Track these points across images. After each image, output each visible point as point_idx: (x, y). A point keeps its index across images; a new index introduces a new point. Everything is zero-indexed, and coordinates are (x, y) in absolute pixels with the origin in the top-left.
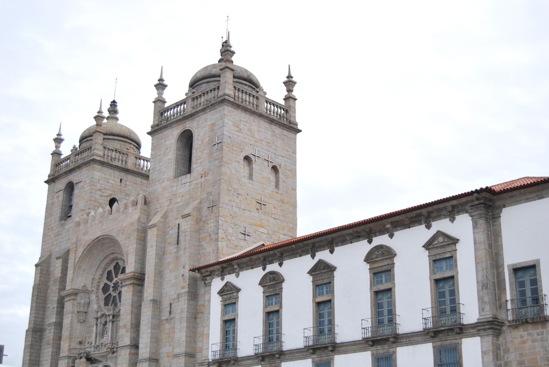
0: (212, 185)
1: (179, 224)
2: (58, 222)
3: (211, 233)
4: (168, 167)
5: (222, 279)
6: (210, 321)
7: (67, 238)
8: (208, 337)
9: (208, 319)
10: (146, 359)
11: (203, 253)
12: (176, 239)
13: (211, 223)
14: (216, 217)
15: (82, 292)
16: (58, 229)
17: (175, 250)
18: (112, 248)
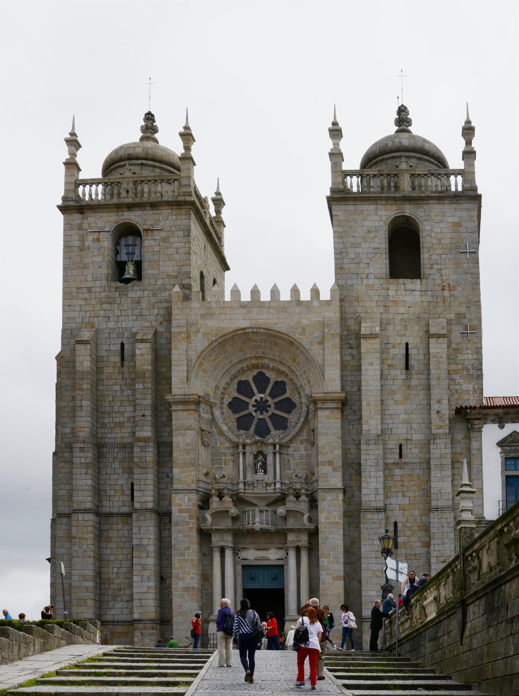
0: (464, 305)
1: (407, 344)
2: (104, 283)
3: (470, 366)
4: (374, 259)
5: (502, 427)
6: (482, 473)
7: (136, 312)
8: (482, 492)
9: (480, 471)
10: (377, 509)
11: (457, 390)
12: (403, 362)
13: (468, 354)
14: (477, 348)
15: (205, 403)
16: (106, 294)
17: (404, 377)
18: (261, 351)
